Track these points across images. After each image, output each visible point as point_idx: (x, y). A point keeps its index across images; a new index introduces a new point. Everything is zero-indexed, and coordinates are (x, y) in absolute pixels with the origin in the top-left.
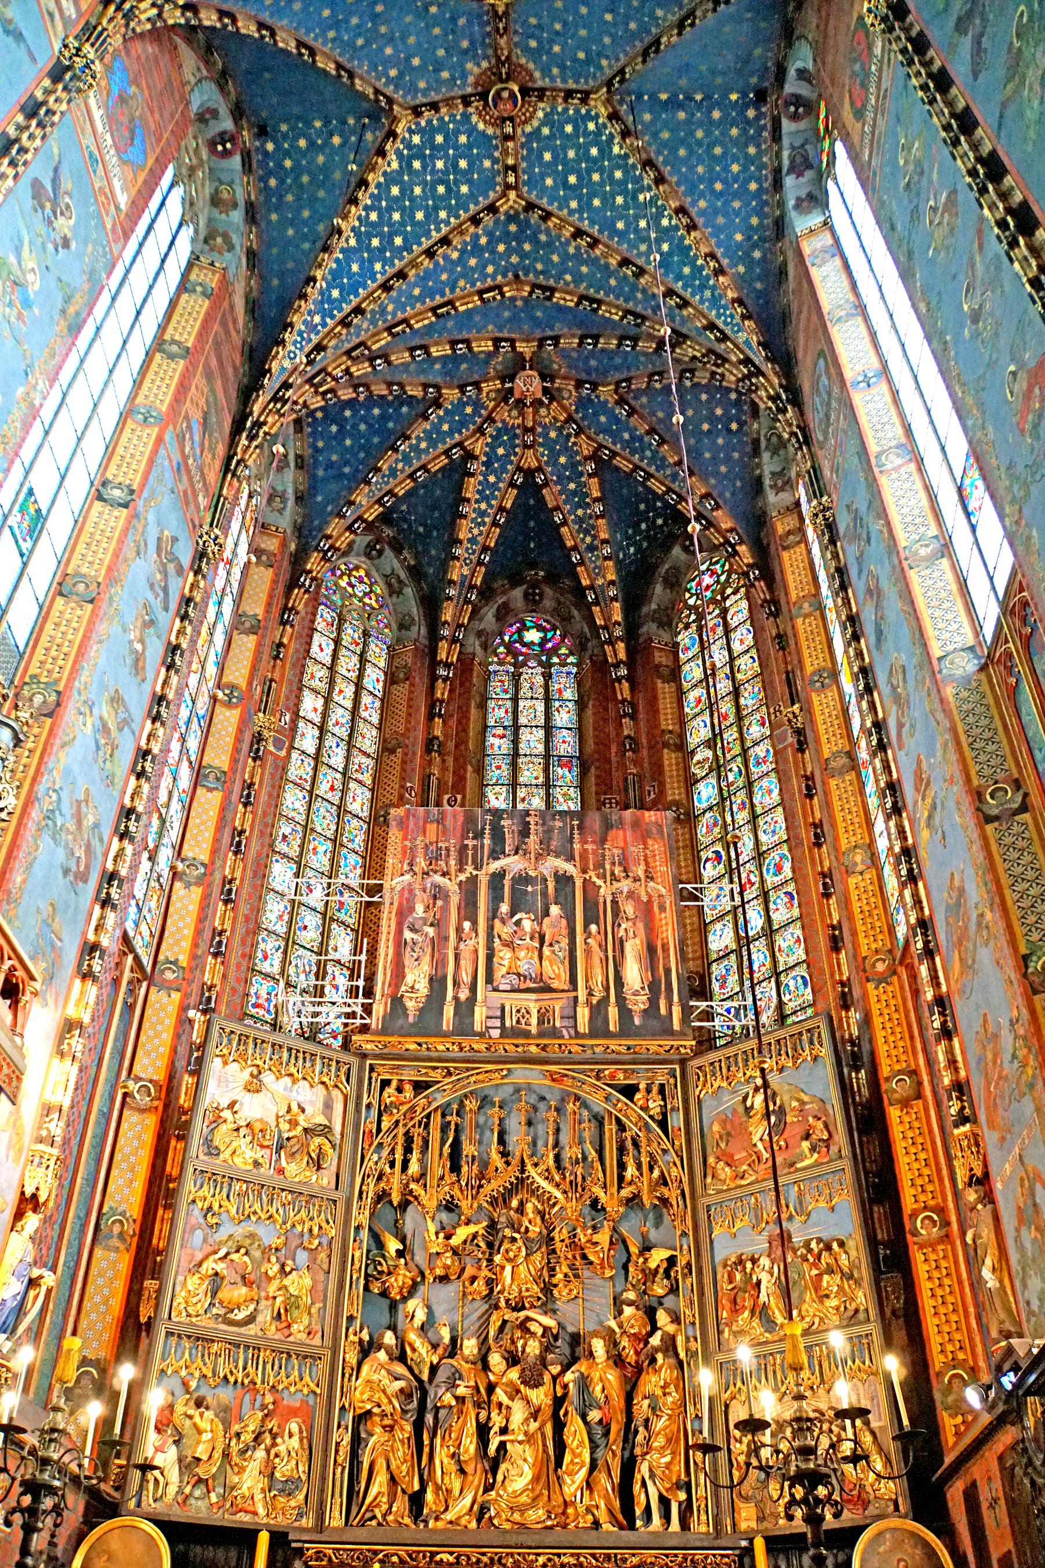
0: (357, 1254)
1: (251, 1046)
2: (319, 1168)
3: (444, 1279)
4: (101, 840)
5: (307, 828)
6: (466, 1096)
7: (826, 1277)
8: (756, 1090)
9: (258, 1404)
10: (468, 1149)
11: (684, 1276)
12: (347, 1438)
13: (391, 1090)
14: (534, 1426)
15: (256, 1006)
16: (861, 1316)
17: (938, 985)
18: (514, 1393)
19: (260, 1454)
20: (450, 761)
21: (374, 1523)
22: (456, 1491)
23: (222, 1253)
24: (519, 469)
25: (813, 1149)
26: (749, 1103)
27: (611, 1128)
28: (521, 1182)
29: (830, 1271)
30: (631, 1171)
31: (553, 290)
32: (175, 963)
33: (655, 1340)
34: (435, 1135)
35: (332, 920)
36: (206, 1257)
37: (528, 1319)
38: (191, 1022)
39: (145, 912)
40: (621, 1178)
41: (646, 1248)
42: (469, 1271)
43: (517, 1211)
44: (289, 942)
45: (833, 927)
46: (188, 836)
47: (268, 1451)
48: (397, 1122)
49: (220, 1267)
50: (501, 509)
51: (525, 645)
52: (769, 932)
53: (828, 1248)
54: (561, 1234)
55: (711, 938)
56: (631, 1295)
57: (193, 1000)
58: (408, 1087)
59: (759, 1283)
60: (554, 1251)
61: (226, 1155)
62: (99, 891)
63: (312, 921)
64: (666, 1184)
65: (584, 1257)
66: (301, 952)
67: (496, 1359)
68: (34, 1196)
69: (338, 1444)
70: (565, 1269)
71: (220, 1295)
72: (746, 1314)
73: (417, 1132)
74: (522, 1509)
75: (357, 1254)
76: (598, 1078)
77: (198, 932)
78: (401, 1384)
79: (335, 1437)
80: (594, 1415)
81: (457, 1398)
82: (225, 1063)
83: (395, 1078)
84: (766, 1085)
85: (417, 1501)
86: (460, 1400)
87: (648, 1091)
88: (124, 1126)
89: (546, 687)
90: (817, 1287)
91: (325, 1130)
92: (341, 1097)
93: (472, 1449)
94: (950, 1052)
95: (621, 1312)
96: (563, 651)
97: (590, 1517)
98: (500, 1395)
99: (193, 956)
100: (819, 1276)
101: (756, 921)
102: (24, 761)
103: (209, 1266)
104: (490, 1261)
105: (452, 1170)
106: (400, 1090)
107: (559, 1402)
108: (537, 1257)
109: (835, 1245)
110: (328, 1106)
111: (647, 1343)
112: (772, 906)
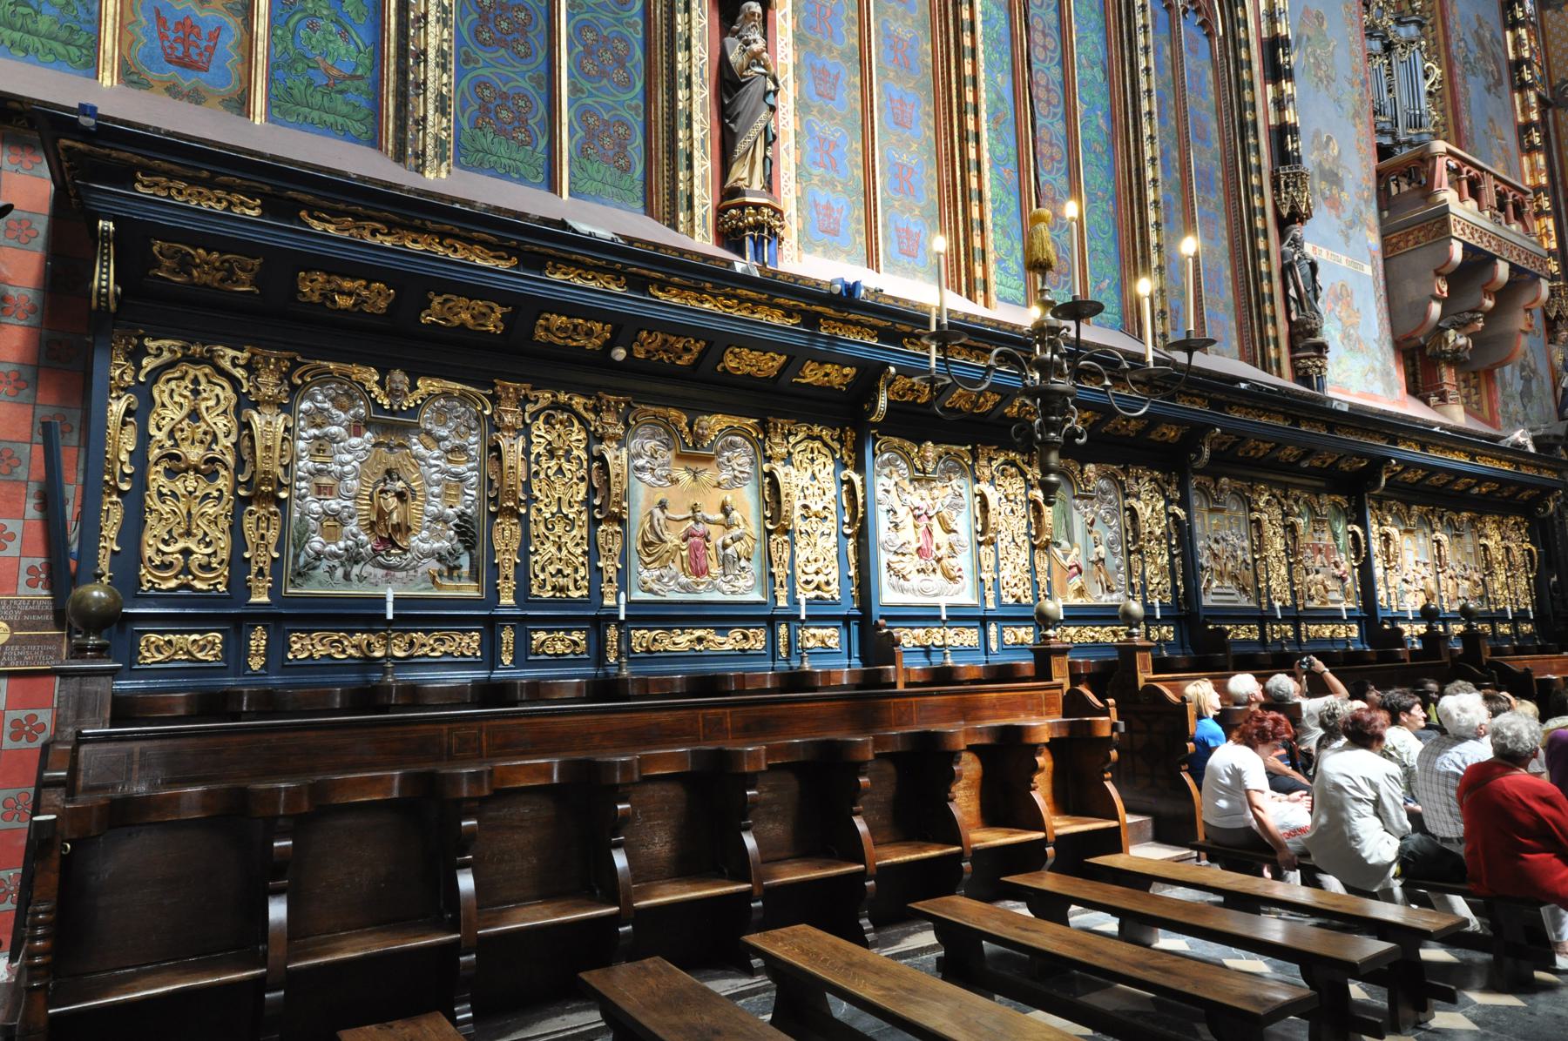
4: (1498, 42)
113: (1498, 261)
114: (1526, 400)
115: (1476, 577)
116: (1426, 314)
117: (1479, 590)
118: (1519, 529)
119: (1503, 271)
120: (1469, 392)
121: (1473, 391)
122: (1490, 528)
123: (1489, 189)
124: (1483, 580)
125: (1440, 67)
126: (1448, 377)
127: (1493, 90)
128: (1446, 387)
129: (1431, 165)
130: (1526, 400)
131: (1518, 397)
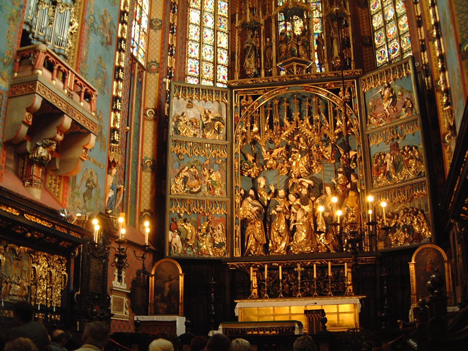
0: (236, 163)
1: (187, 90)
2: (219, 133)
3: (270, 169)
4: (114, 27)
6: (273, 99)
7: (410, 160)
8: (386, 88)
9: (206, 220)
10: (276, 120)
11: (359, 162)
12: (239, 228)
13: (244, 100)
14: (305, 219)
15: (191, 71)
16: (423, 174)
17: (441, 50)
19: (209, 236)
21: (251, 255)
22: (279, 243)
23: (187, 168)
25: (406, 111)
26: (382, 93)
28: (297, 131)
29: (412, 158)
32: (155, 62)
33: (349, 186)
34: (262, 115)
35: (217, 31)
36: (181, 171)
37: (302, 181)
38: (165, 83)
39: (140, 45)
40: (335, 125)
42: (280, 166)
43: (297, 141)
44: (201, 43)
45: (419, 17)
46: (153, 10)
47: (211, 234)
48: (247, 112)
49: (186, 174)
52: (397, 18)
53: (411, 149)
55: (373, 21)
56: (341, 170)
57: (164, 74)
58: (250, 98)
59: (386, 163)
60: (312, 155)
62: (117, 46)
63: (209, 33)
64: (352, 127)
65: (323, 157)
66: (207, 46)
67: (292, 197)
68: (113, 161)
69: (236, 230)
70: (316, 162)
71: (187, 183)
72: (382, 174)
75: (236, 163)
76: (324, 88)
77: (162, 48)
78: (257, 208)
79: (235, 228)
81: (277, 212)
82: (178, 98)
83: (245, 95)
84: (389, 86)
85: (266, 246)
86: (279, 212)
87: (344, 90)
88: (146, 127)
90: (407, 164)
91: (219, 119)
92: (224, 105)
93: (284, 228)
94: (444, 77)
95: (337, 176)
97: (326, 249)
98: (293, 209)
99: (162, 58)
100: (408, 160)
101: (390, 14)
102: (78, 8)
103: (182, 175)
104: (288, 160)
105: (270, 128)
106: (247, 100)
108: (305, 158)
109: (414, 148)
110: (220, 109)
111: (346, 187)
112: (397, 7)
113: (65, 116)
114: (86, 198)
115: (25, 284)
116: (18, 131)
117: (25, 293)
118: (62, 263)
119: (67, 122)
120: (56, 186)
121: (57, 186)
122: (42, 260)
123: (70, 79)
124: (28, 287)
125: (78, 22)
126: (36, 171)
127: (105, 45)
128: (34, 178)
129: (37, 54)
130: (86, 198)
131: (82, 196)
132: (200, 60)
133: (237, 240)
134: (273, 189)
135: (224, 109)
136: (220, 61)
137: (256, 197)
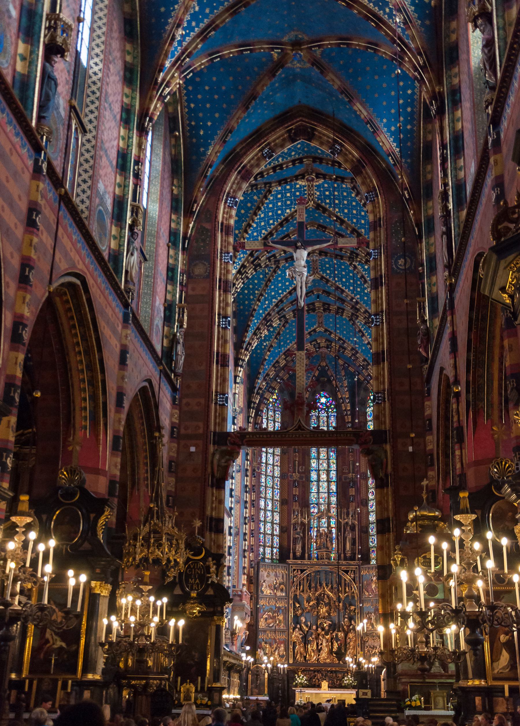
5: (266, 487)
18: (323, 637)
20: (301, 454)
24: (320, 365)
27: (343, 581)
30: (347, 589)
31: (332, 342)
33: (351, 627)
34: (305, 581)
41: (351, 605)
50: (314, 376)
51: (322, 404)
54: (332, 602)
61: (265, 593)
63: (269, 514)
67: (319, 629)
73: (302, 582)
74: (325, 659)
80: (339, 642)
85: (305, 657)
89: (327, 421)
96: (332, 406)
107: (332, 639)
132: (265, 534)
133: (291, 653)
134: (309, 624)
135: (285, 576)
136: (275, 533)
137: (301, 629)
